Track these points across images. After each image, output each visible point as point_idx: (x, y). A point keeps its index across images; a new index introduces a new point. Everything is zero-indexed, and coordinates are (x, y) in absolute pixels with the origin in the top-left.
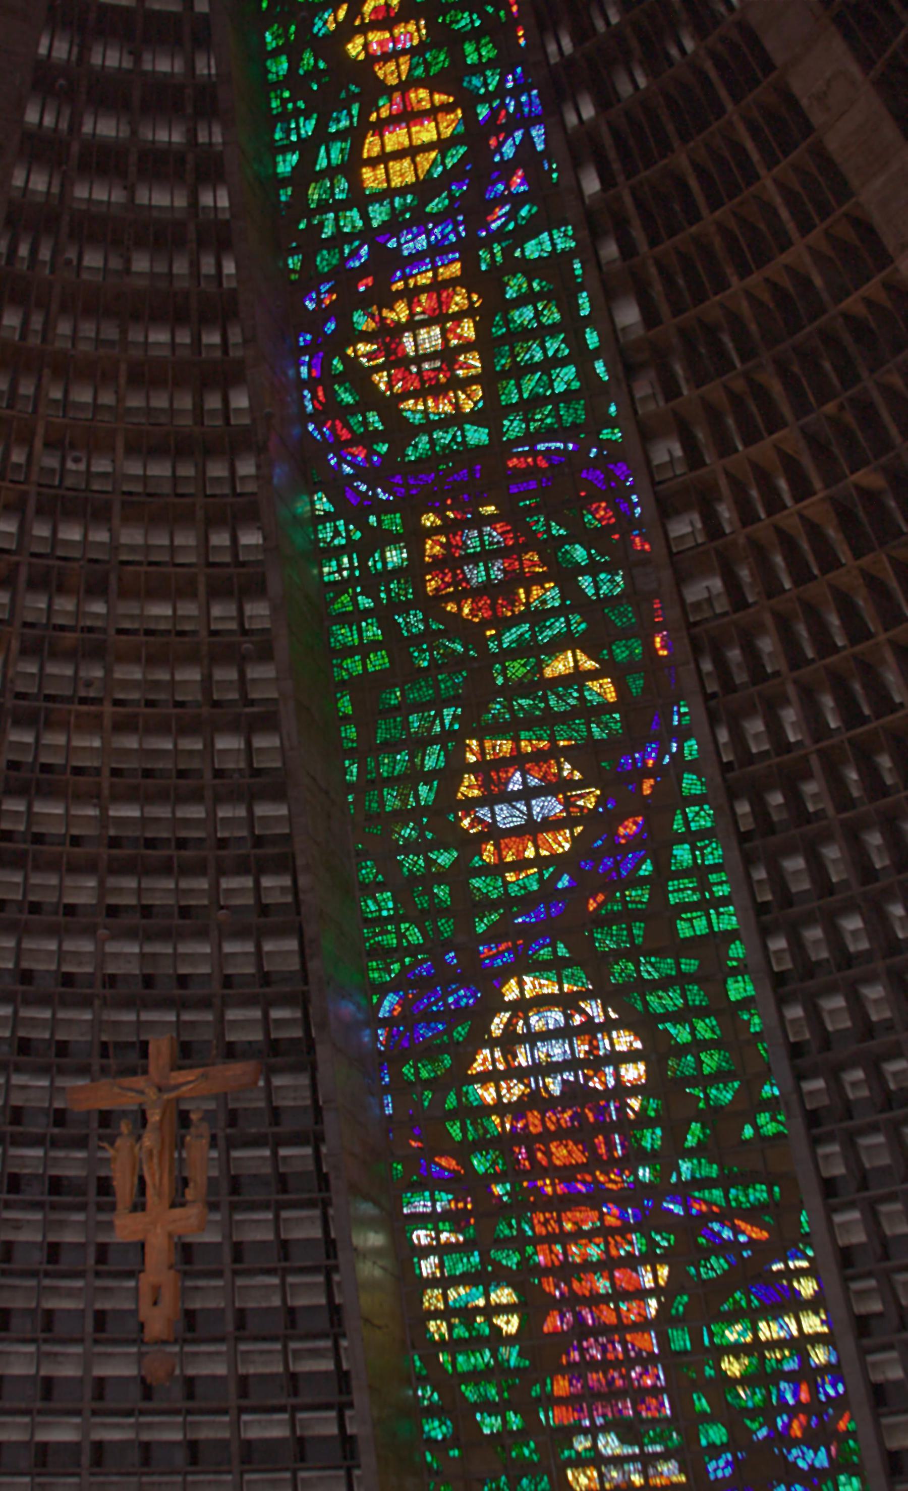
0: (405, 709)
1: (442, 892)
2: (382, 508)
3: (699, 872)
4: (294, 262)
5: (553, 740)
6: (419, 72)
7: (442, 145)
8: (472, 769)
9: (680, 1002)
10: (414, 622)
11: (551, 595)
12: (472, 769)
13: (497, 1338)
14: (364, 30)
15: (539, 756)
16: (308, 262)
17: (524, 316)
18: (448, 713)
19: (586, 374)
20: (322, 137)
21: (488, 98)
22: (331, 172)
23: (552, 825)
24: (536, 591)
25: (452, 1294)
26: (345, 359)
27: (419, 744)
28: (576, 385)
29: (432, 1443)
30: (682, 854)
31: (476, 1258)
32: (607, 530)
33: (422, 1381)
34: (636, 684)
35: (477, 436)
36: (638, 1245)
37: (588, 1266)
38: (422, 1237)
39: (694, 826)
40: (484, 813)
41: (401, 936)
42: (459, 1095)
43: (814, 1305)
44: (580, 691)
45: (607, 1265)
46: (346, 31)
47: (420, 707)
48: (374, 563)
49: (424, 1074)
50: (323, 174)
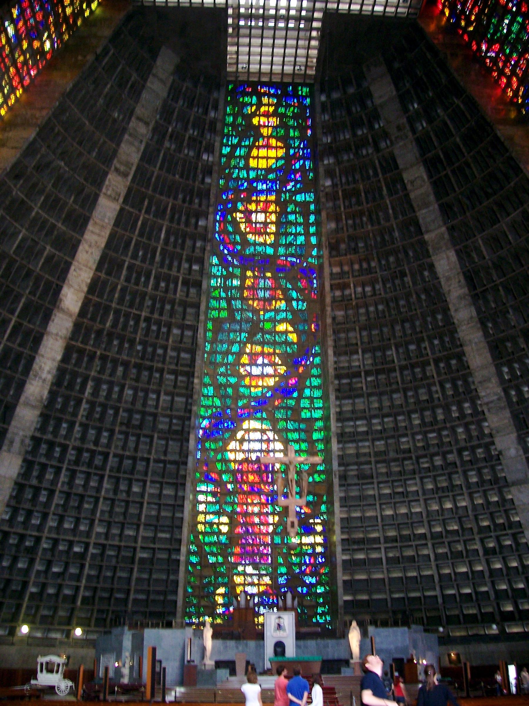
0: (230, 331)
1: (230, 391)
2: (234, 266)
3: (311, 399)
4: (222, 182)
5: (274, 350)
6: (274, 134)
7: (277, 159)
8: (248, 354)
9: (298, 437)
10: (237, 304)
11: (282, 305)
12: (248, 354)
13: (220, 533)
14: (259, 116)
15: (269, 354)
16: (227, 183)
17: (292, 218)
18: (243, 335)
19: (307, 240)
20: (239, 145)
21: (294, 148)
22: (240, 157)
23: (268, 376)
24: (278, 302)
25: (207, 516)
26: (232, 217)
27: (232, 343)
28: (304, 243)
29: (192, 564)
30: (307, 392)
31: (217, 507)
32: (305, 289)
33: (192, 543)
34: (304, 338)
35: (270, 251)
36: (270, 509)
37: (253, 514)
38: (201, 498)
39: (313, 385)
40: (248, 368)
41: (213, 402)
42: (222, 455)
43: (320, 534)
44: (286, 337)
45: (259, 514)
46: (254, 115)
47: (235, 331)
48: (228, 283)
49: (213, 447)
50: (237, 157)
